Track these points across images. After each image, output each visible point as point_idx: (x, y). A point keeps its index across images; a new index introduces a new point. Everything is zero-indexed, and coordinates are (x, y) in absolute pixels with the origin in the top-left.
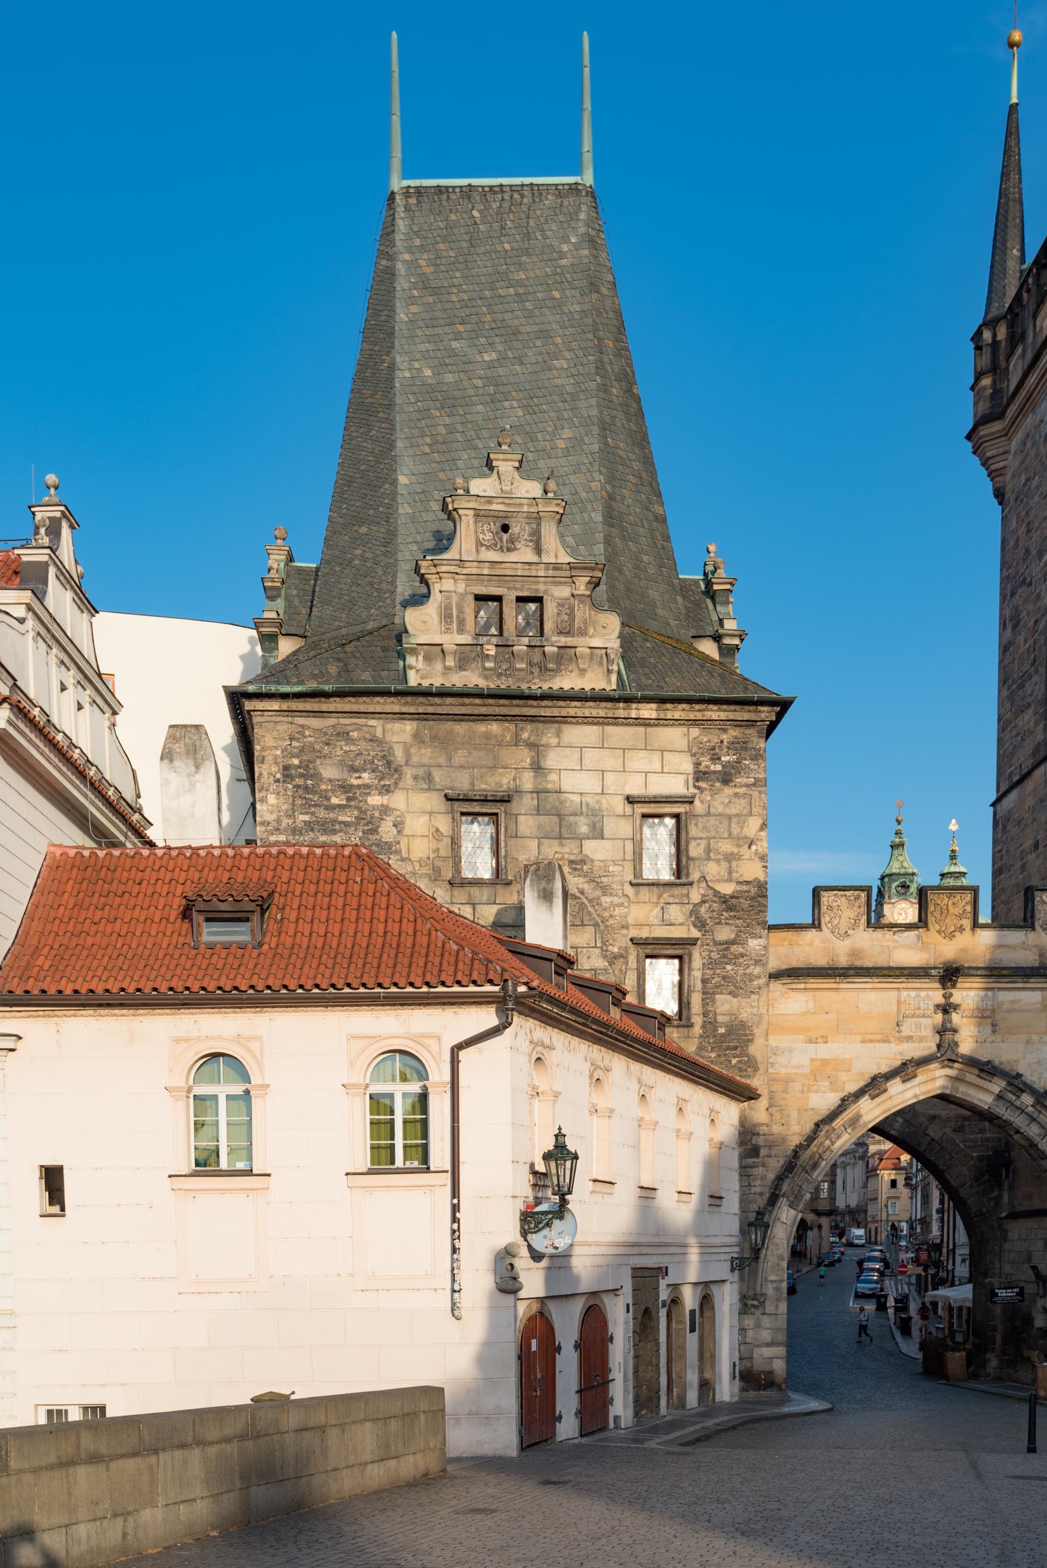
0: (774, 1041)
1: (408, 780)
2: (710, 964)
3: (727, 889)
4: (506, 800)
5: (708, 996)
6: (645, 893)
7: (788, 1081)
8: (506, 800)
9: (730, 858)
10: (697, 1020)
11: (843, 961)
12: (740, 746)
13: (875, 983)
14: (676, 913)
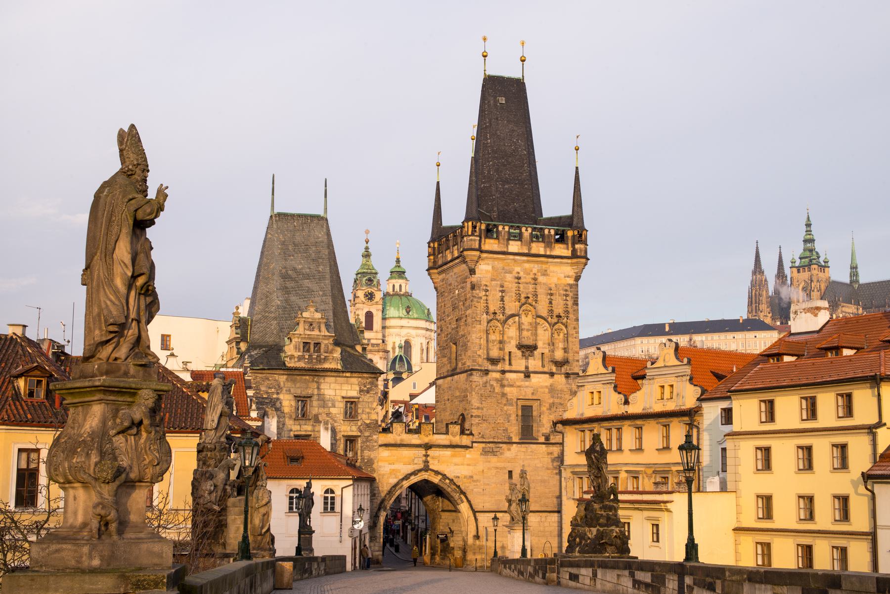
0: (380, 464)
1: (284, 391)
2: (363, 442)
3: (368, 422)
4: (310, 397)
5: (362, 451)
6: (346, 423)
7: (383, 475)
8: (310, 397)
9: (369, 413)
10: (359, 458)
11: (399, 442)
12: (372, 383)
13: (407, 448)
14: (354, 428)
